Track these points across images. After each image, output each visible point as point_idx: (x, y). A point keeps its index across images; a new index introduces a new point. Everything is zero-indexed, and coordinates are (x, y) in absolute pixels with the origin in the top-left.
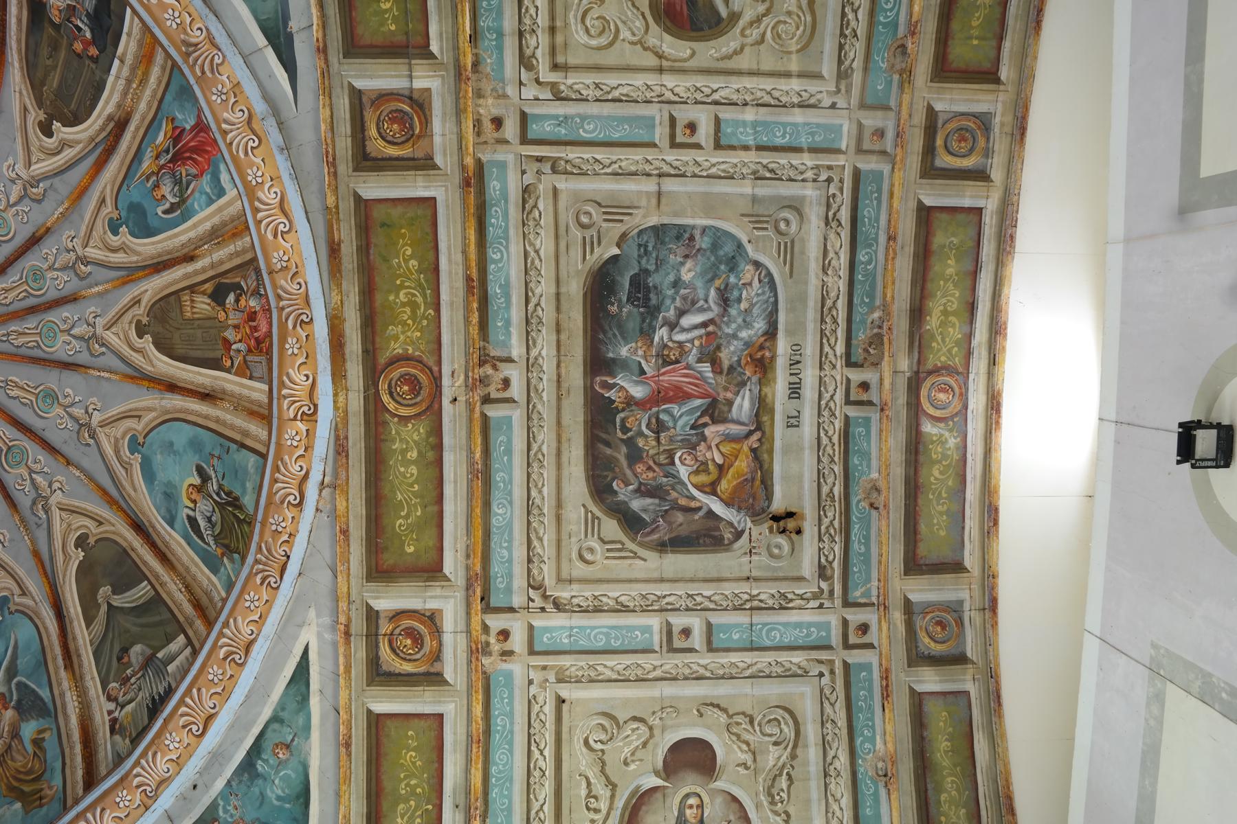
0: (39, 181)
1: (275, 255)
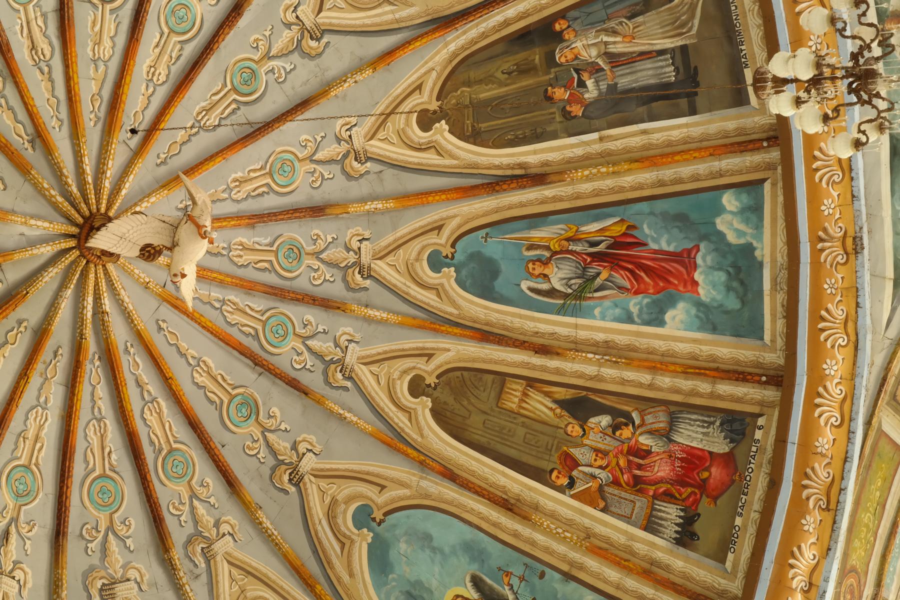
0: (369, 159)
1: (820, 439)
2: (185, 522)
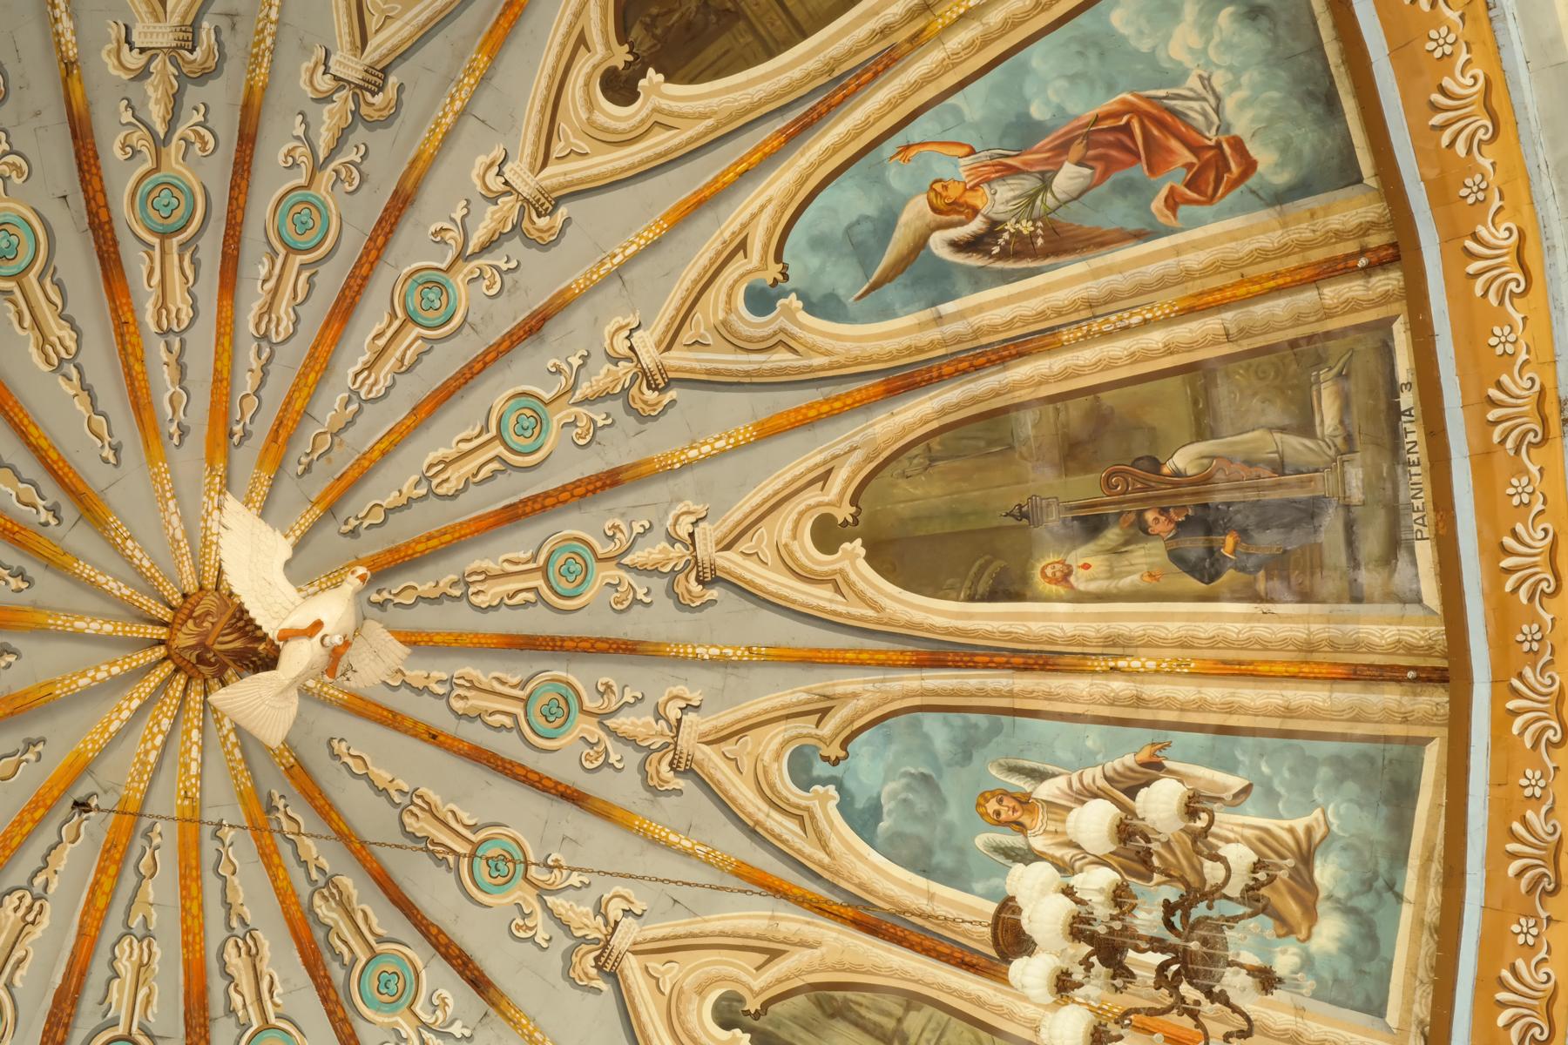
2: (198, 111)
